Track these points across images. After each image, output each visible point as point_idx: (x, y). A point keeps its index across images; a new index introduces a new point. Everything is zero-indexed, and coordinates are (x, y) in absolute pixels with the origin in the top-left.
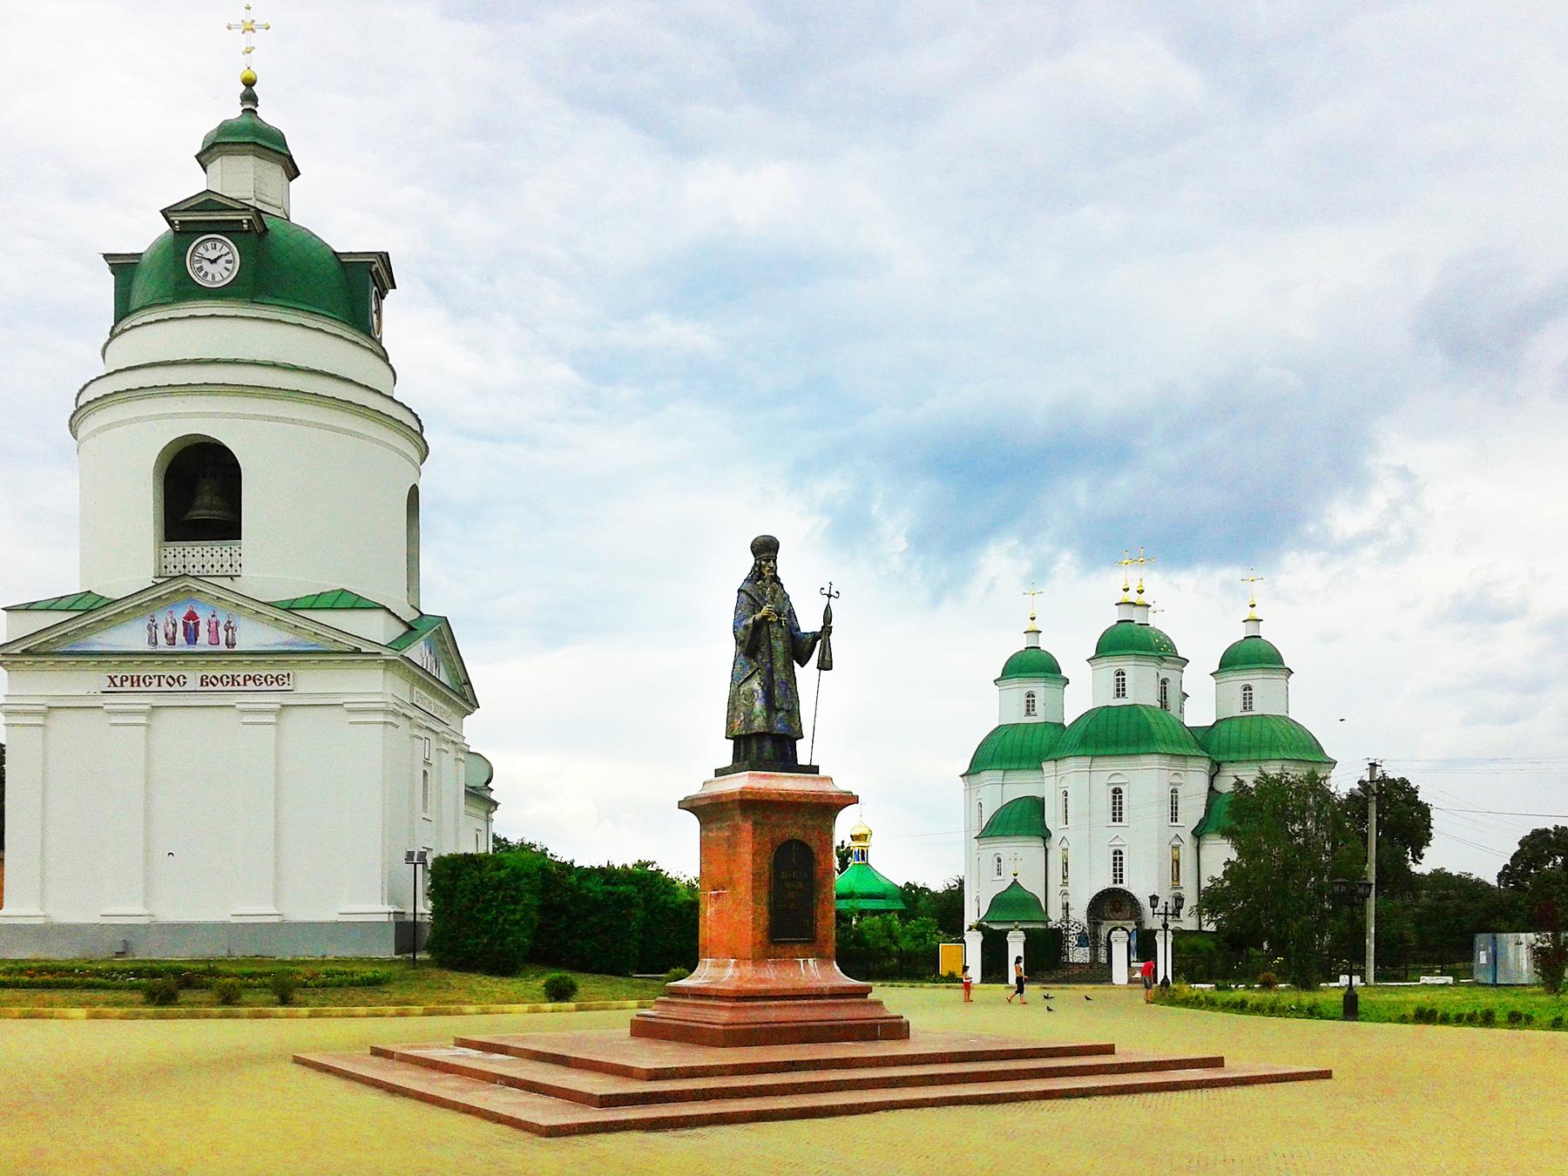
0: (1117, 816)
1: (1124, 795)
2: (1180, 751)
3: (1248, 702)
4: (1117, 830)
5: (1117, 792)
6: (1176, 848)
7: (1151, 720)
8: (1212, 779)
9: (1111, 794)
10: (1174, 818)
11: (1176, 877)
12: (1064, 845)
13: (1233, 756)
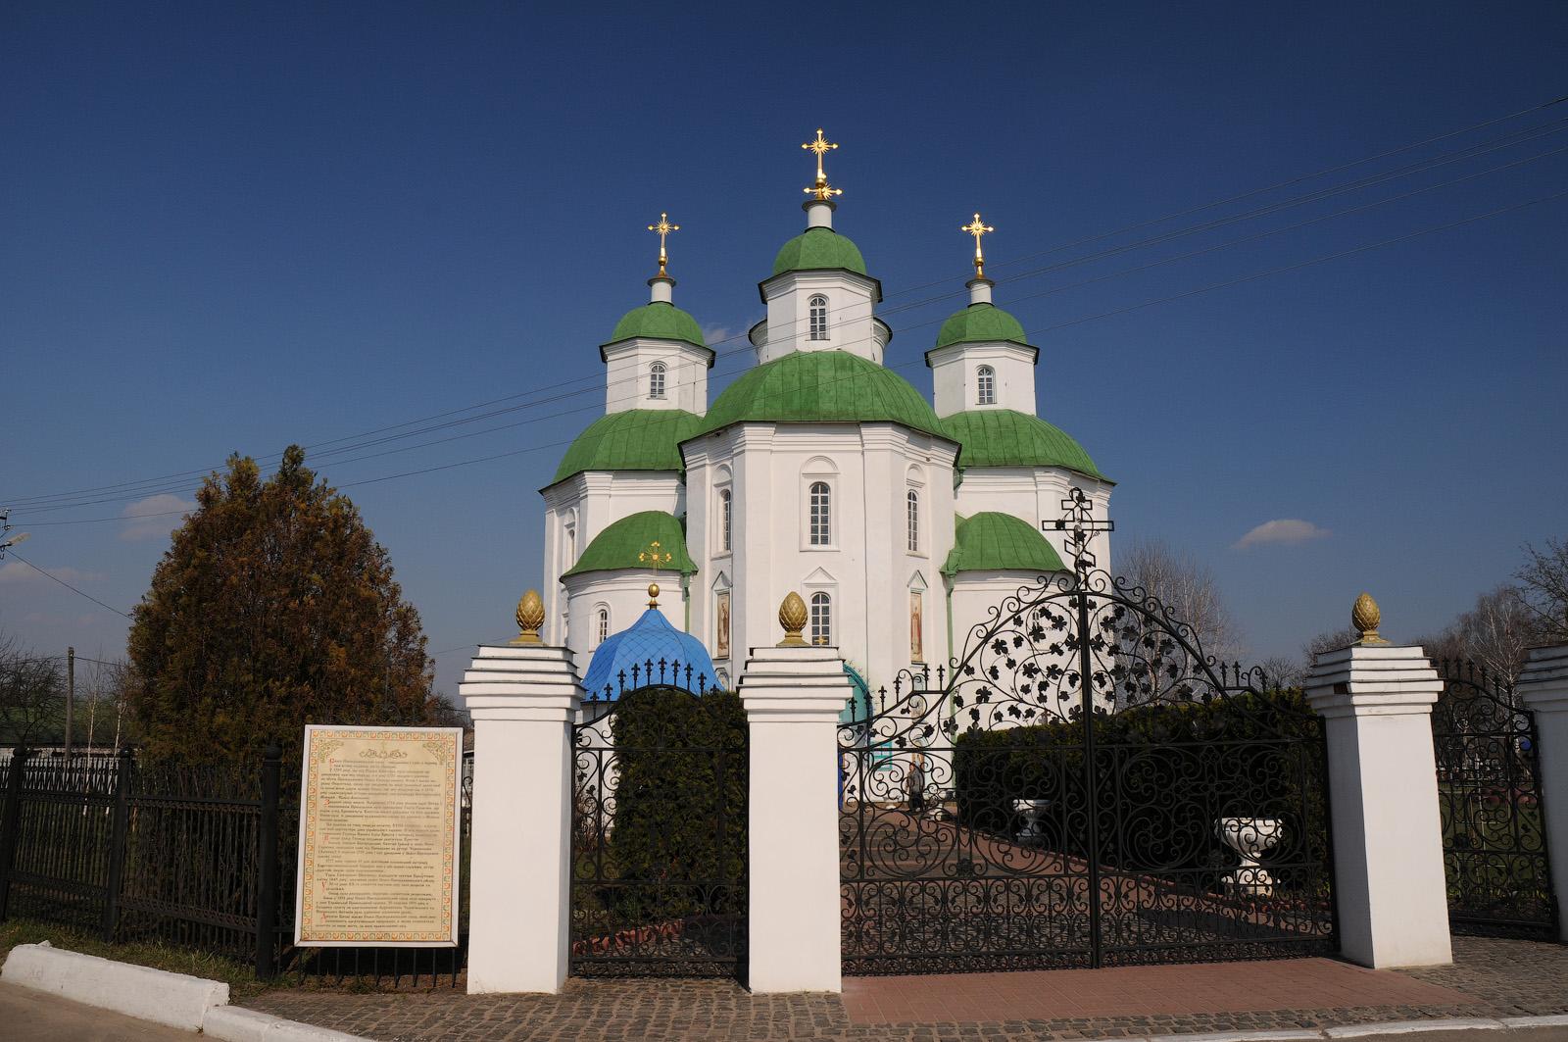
0: (820, 532)
1: (832, 496)
3: (986, 391)
4: (820, 555)
5: (820, 488)
8: (955, 489)
9: (808, 494)
10: (913, 545)
11: (918, 646)
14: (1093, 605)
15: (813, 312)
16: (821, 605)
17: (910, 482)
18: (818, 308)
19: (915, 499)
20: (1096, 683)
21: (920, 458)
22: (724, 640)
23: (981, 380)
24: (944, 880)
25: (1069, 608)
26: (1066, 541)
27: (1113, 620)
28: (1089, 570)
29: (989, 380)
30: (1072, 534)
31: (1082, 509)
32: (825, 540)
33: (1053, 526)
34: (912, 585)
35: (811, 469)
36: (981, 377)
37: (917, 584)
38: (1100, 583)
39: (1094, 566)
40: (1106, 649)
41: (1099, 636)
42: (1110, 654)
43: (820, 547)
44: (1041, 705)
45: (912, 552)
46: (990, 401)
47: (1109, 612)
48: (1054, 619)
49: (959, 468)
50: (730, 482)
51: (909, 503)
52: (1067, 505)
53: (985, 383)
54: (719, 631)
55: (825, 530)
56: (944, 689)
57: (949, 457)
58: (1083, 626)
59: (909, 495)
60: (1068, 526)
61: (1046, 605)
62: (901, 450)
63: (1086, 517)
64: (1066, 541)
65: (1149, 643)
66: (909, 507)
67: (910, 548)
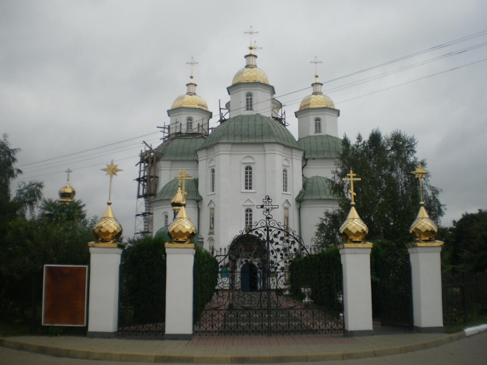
0: (249, 185)
1: (253, 171)
2: (287, 144)
5: (249, 169)
6: (286, 209)
7: (270, 124)
8: (303, 168)
9: (244, 171)
12: (212, 206)
13: (314, 156)
14: (271, 230)
15: (247, 99)
16: (249, 213)
17: (283, 165)
18: (249, 97)
19: (286, 172)
20: (271, 253)
21: (288, 156)
22: (212, 226)
23: (316, 123)
24: (225, 310)
25: (264, 231)
26: (264, 211)
27: (277, 235)
28: (270, 220)
29: (319, 123)
30: (265, 209)
31: (269, 202)
32: (250, 188)
33: (260, 207)
34: (284, 205)
35: (245, 161)
36: (316, 122)
37: (286, 205)
38: (273, 224)
39: (272, 219)
40: (274, 243)
41: (272, 240)
42: (276, 245)
43: (249, 191)
44: (255, 260)
45: (285, 192)
46: (320, 131)
47: (276, 232)
48: (259, 234)
49: (305, 160)
50: (214, 166)
51: (284, 174)
52: (264, 201)
53: (318, 124)
54: (210, 223)
55: (251, 184)
56: (226, 255)
57: (300, 155)
58: (268, 238)
59: (284, 171)
60: (264, 207)
61: (257, 230)
62: (280, 153)
63: (270, 204)
64: (264, 211)
65: (288, 241)
66: (284, 175)
67: (284, 191)
